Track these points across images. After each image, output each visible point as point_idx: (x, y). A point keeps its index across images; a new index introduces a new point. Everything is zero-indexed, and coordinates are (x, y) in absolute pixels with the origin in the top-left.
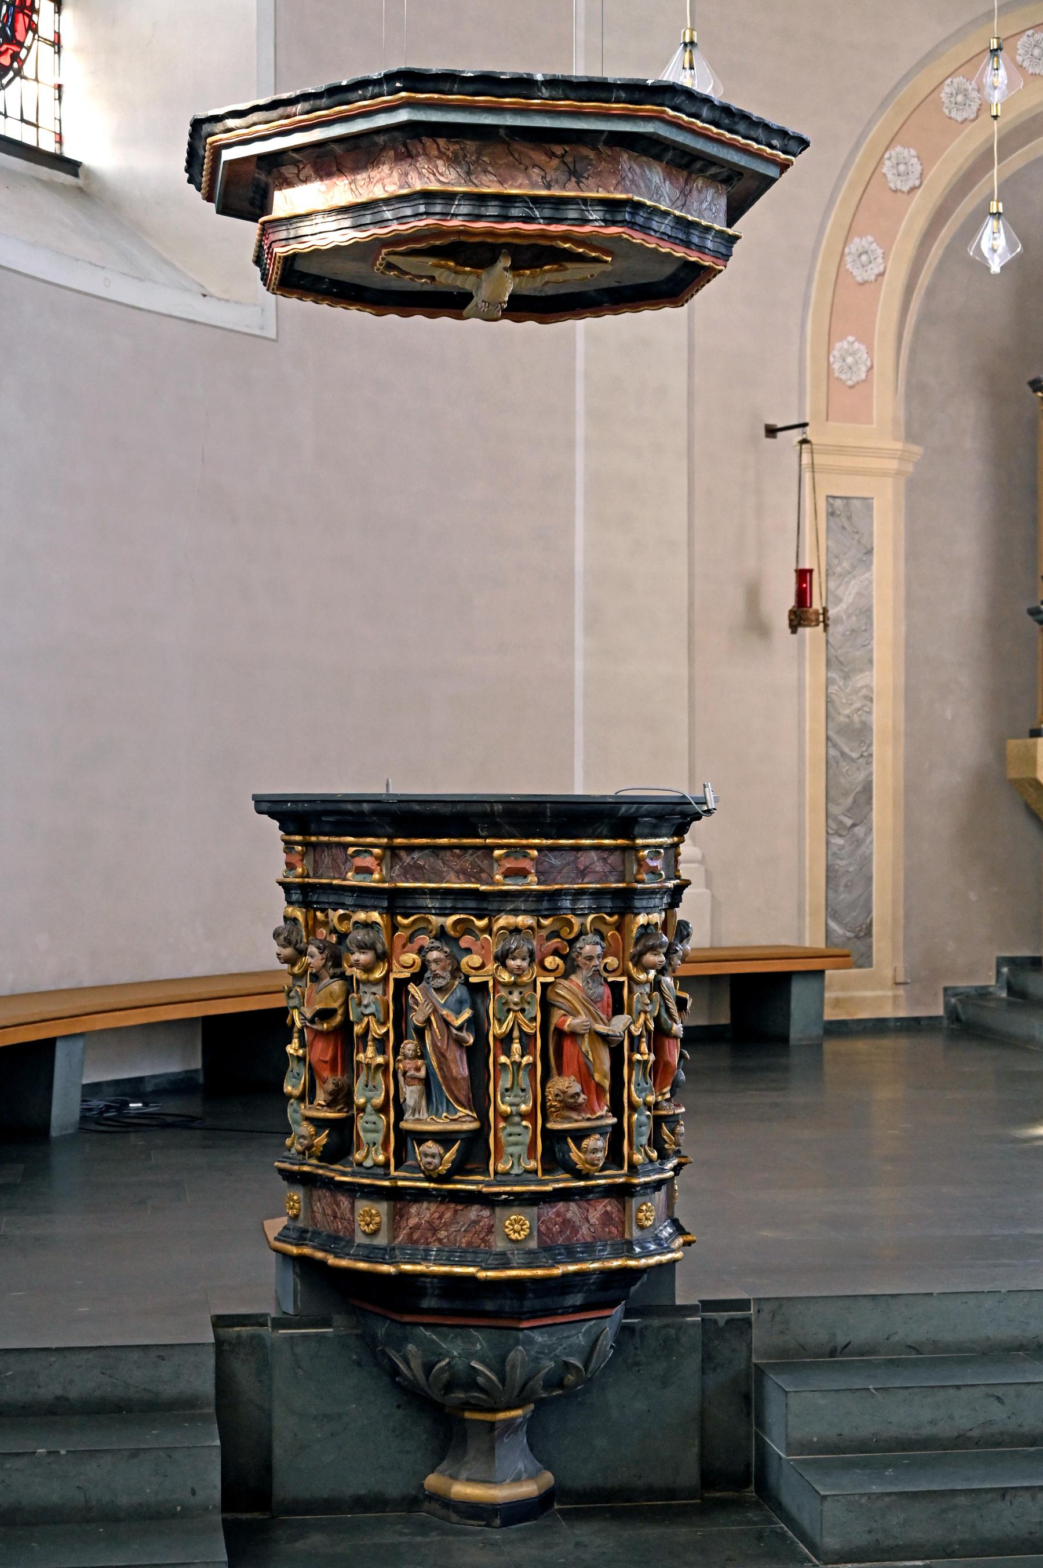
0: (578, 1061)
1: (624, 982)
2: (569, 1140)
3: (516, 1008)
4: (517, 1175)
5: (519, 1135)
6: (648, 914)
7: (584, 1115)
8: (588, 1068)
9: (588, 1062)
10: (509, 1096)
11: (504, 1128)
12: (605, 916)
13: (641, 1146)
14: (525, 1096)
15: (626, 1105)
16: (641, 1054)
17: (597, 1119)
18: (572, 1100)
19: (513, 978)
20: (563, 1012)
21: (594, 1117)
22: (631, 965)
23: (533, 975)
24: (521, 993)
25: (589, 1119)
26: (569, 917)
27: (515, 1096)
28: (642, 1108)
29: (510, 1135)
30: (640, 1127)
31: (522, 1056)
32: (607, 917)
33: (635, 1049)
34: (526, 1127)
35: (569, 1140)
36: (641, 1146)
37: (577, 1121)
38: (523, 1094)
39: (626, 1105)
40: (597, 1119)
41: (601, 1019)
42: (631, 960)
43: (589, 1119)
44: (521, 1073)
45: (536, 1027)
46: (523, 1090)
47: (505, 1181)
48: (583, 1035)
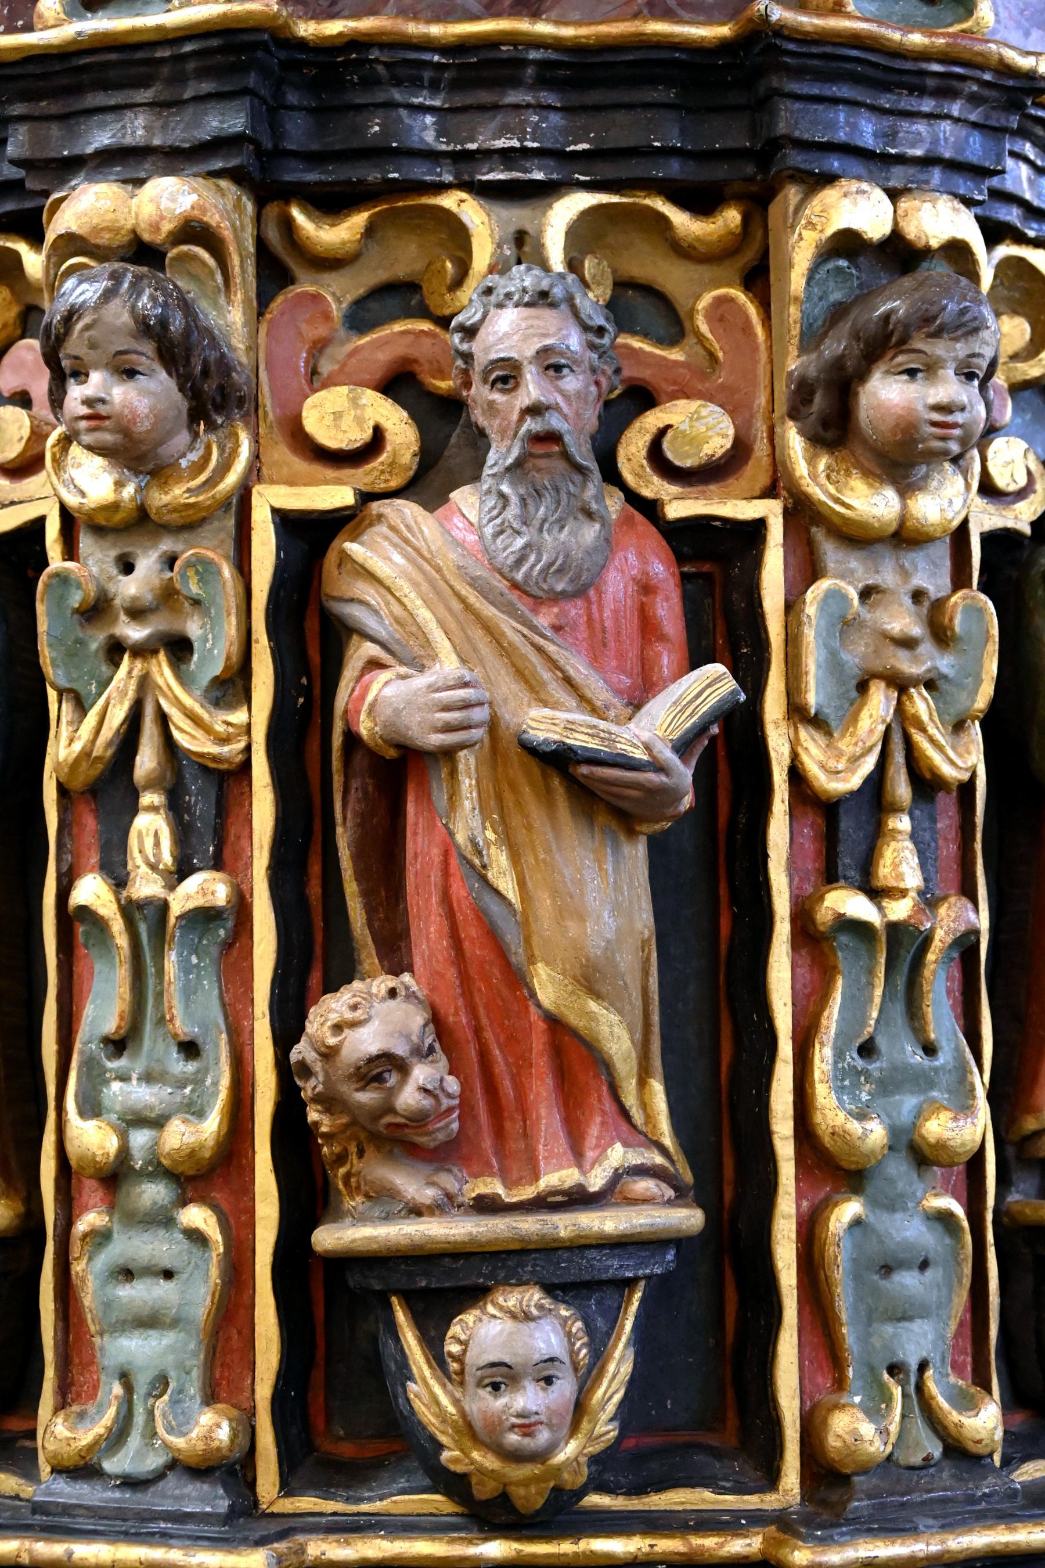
0: (446, 898)
1: (759, 526)
2: (401, 1317)
3: (135, 633)
4: (131, 1483)
5: (168, 1274)
6: (894, 195)
7: (448, 1181)
8: (493, 936)
9: (495, 908)
10: (124, 1078)
11: (100, 1237)
12: (661, 205)
13: (895, 1369)
14: (197, 1080)
15: (785, 1149)
16: (876, 894)
17: (541, 1204)
18: (366, 1097)
19: (129, 491)
20: (370, 650)
21: (527, 1193)
22: (795, 442)
23: (225, 467)
24: (170, 561)
25: (487, 1206)
26: (449, 201)
27: (148, 1078)
28: (899, 1169)
29: (127, 1273)
30: (887, 1270)
31: (182, 871)
32: (679, 219)
33: (846, 861)
34: (197, 1237)
35: (401, 1317)
36: (895, 1369)
37: (416, 1211)
38: (191, 1067)
39: (785, 1149)
40: (541, 1204)
41: (568, 681)
42: (793, 414)
43: (487, 1206)
44: (171, 961)
45: (248, 729)
46: (190, 1049)
47: (67, 1510)
48: (449, 754)
